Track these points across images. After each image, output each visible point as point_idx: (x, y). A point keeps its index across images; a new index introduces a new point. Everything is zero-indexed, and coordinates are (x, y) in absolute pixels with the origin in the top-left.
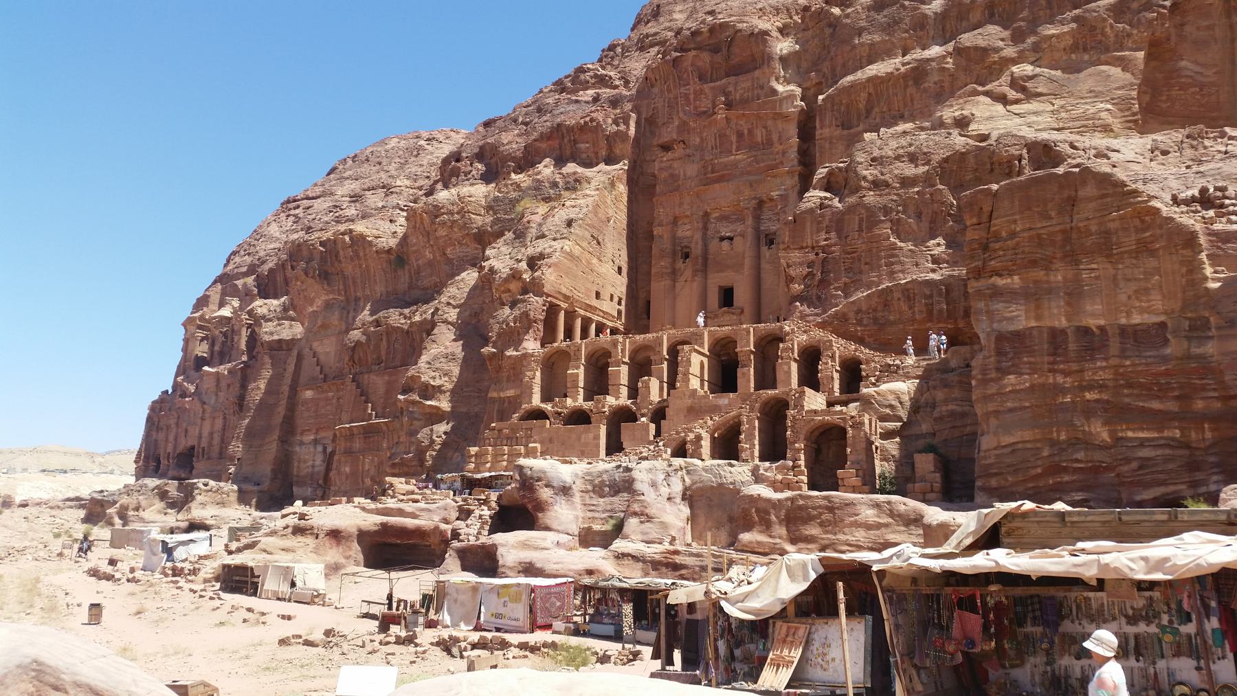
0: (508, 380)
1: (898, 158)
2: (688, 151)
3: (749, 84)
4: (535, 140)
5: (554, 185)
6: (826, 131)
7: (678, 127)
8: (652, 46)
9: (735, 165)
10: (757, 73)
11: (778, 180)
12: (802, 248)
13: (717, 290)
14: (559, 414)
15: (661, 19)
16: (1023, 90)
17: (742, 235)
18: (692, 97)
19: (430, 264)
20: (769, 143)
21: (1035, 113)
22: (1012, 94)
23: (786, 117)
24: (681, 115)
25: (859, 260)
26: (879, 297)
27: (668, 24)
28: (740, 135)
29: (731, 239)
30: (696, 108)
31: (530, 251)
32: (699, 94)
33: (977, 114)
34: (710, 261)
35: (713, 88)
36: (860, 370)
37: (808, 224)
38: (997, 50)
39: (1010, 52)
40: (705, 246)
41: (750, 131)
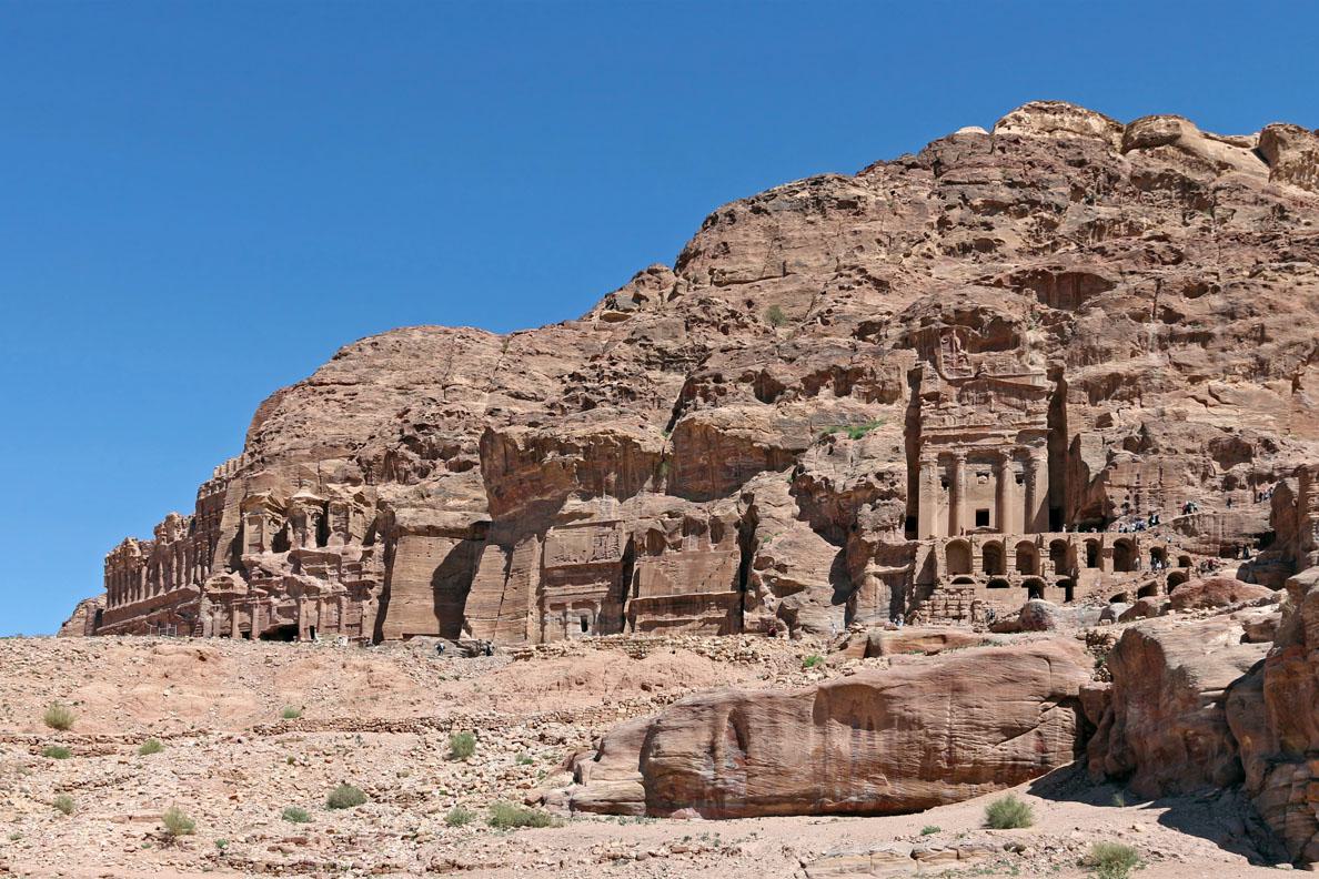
1: (1181, 435)
2: (950, 404)
4: (810, 376)
8: (728, 283)
12: (1120, 486)
14: (983, 582)
15: (735, 259)
16: (1217, 398)
19: (703, 469)
21: (1227, 416)
22: (1211, 400)
27: (745, 266)
28: (999, 396)
33: (1190, 411)
38: (1200, 368)
39: (1205, 371)
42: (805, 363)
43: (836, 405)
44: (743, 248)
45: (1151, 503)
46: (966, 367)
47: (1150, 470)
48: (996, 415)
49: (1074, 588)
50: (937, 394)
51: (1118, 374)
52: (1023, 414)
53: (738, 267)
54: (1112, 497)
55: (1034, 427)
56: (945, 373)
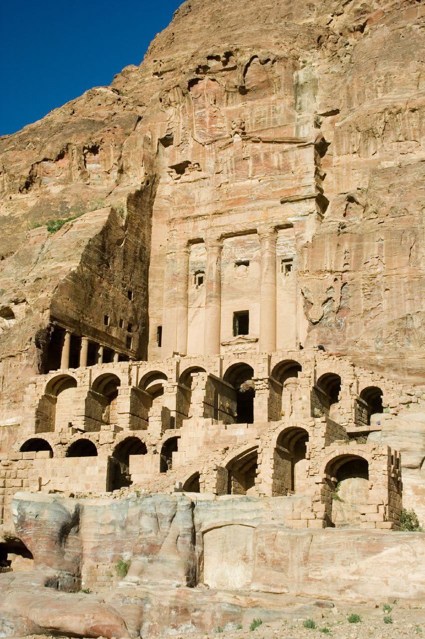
0: (9, 408)
2: (202, 174)
3: (266, 109)
5: (63, 204)
6: (343, 159)
7: (193, 149)
9: (250, 190)
10: (273, 98)
11: (296, 205)
12: (320, 272)
13: (231, 317)
15: (176, 48)
17: (260, 261)
18: (207, 120)
20: (285, 168)
23: (302, 144)
24: (196, 137)
25: (379, 287)
26: (399, 324)
28: (257, 159)
29: (246, 264)
30: (211, 129)
31: (36, 272)
32: (213, 117)
34: (224, 287)
35: (228, 112)
36: (381, 401)
37: (327, 249)
40: (219, 272)
41: (267, 156)
42: (43, 147)
43: (63, 192)
44: (185, 36)
45: (368, 296)
46: (220, 125)
47: (366, 244)
48: (255, 182)
49: (174, 453)
50: (188, 162)
51: (395, 107)
52: (286, 176)
53: (176, 55)
54: (308, 290)
55: (298, 193)
56: (196, 137)
